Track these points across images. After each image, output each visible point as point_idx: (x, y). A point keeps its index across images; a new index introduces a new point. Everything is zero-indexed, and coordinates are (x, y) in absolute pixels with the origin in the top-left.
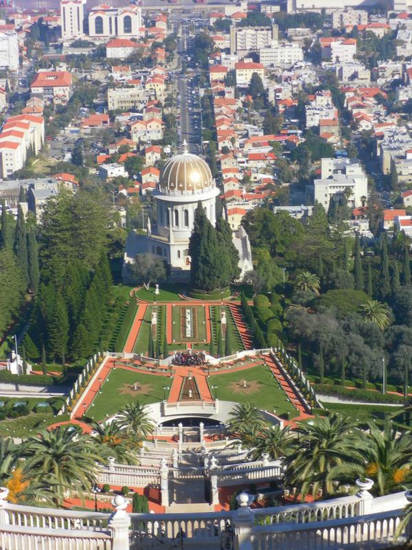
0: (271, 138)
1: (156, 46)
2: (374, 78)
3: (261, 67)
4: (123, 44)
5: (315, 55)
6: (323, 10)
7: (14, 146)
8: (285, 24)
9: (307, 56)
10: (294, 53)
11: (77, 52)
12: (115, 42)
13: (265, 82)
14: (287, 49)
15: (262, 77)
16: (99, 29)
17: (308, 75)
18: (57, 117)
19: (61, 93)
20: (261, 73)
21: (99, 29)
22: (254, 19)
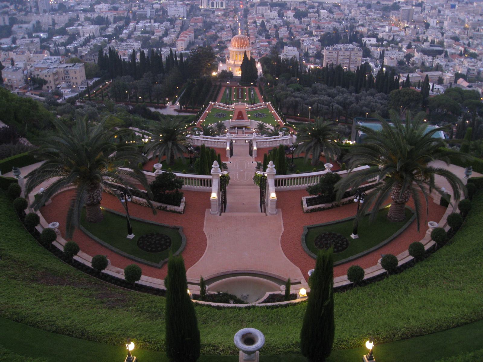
0: (268, 40)
1: (231, 11)
2: (301, 23)
3: (265, 18)
4: (220, 10)
5: (281, 15)
6: (285, 2)
7: (184, 40)
8: (273, 5)
9: (279, 16)
10: (275, 14)
11: (206, 13)
12: (218, 10)
13: (266, 23)
14: (273, 13)
15: (265, 22)
16: (213, 6)
17: (279, 21)
18: (197, 32)
19: (200, 25)
20: (265, 20)
21: (213, 6)
22: (262, 4)
